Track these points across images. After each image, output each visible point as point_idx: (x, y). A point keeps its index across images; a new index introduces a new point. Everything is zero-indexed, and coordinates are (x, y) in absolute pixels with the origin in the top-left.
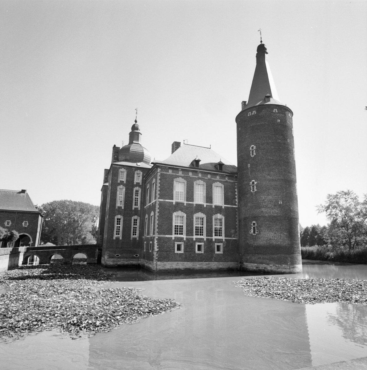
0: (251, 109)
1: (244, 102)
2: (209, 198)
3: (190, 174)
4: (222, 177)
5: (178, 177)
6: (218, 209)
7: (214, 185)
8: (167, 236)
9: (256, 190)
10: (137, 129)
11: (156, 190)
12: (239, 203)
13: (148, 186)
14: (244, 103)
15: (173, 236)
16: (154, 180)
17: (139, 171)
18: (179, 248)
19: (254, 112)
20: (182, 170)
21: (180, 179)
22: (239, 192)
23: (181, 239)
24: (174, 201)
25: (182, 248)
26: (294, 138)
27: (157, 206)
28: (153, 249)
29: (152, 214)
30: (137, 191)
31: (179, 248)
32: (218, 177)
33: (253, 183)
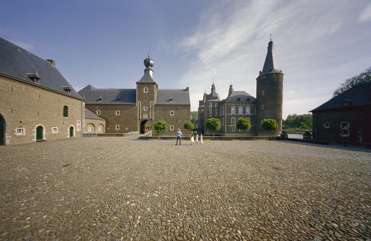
0: (263, 76)
1: (261, 71)
2: (244, 112)
3: (237, 104)
4: (249, 103)
5: (232, 105)
6: (248, 116)
7: (246, 107)
8: (229, 126)
9: (263, 108)
10: (214, 86)
11: (225, 110)
12: (256, 113)
13: (220, 108)
14: (260, 72)
15: (231, 126)
16: (224, 107)
17: (216, 103)
18: (233, 129)
19: (265, 77)
20: (234, 103)
21: (234, 106)
22: (256, 109)
23: (234, 127)
24: (231, 114)
25: (235, 129)
26: (283, 86)
27: (226, 116)
28: (225, 130)
29: (223, 118)
30: (216, 110)
31: (233, 129)
32: (248, 104)
33: (263, 106)
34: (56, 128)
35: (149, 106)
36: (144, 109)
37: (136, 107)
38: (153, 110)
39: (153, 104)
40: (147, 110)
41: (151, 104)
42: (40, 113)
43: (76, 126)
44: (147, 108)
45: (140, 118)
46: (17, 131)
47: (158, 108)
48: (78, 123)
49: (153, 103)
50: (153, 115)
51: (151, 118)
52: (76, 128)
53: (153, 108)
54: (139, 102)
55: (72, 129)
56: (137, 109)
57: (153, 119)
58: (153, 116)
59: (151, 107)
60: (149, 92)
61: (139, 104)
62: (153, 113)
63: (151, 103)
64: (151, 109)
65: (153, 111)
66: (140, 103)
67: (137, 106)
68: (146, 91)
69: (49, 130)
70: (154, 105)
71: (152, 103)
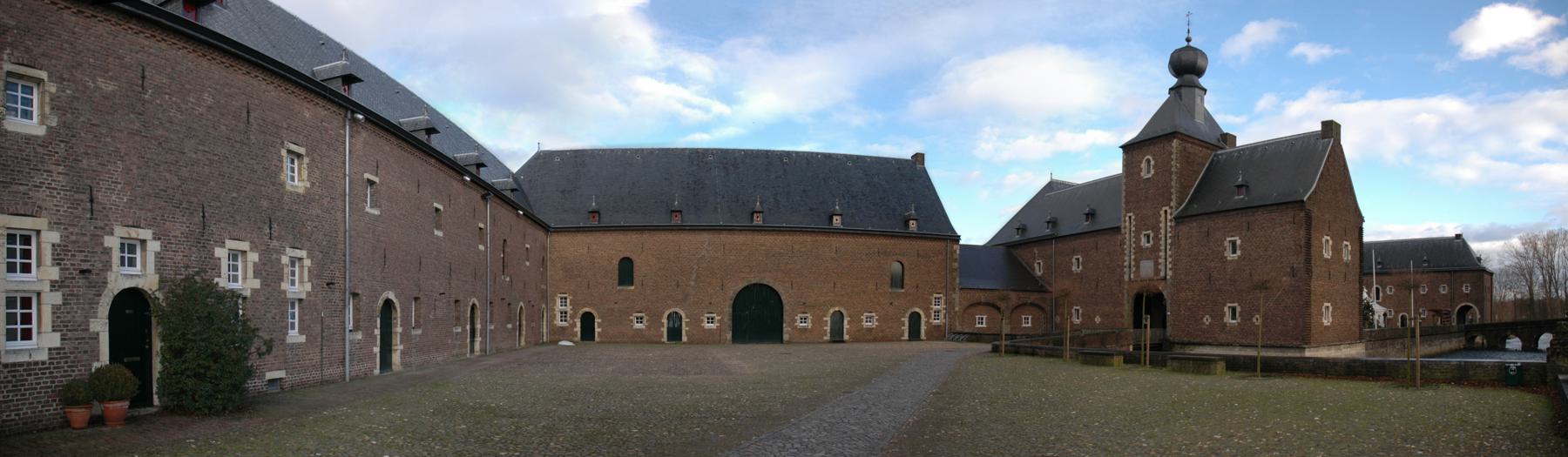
34: (874, 314)
35: (1156, 229)
36: (1143, 240)
37: (1120, 237)
38: (1169, 241)
39: (1169, 217)
40: (1152, 242)
41: (1162, 219)
42: (839, 285)
43: (927, 310)
44: (1152, 235)
45: (1132, 277)
46: (865, 320)
47: (1184, 229)
48: (934, 303)
49: (1169, 211)
50: (1169, 260)
51: (1162, 274)
52: (928, 316)
53: (1169, 235)
54: (1130, 217)
55: (915, 318)
56: (1122, 243)
57: (1168, 277)
58: (1169, 266)
59: (1163, 231)
60: (1156, 174)
61: (1127, 224)
62: (1169, 253)
63: (1162, 213)
64: (1163, 239)
65: (1168, 247)
66: (1133, 217)
67: (1123, 231)
68: (1149, 172)
69: (855, 320)
70: (1171, 220)
71: (1166, 211)
